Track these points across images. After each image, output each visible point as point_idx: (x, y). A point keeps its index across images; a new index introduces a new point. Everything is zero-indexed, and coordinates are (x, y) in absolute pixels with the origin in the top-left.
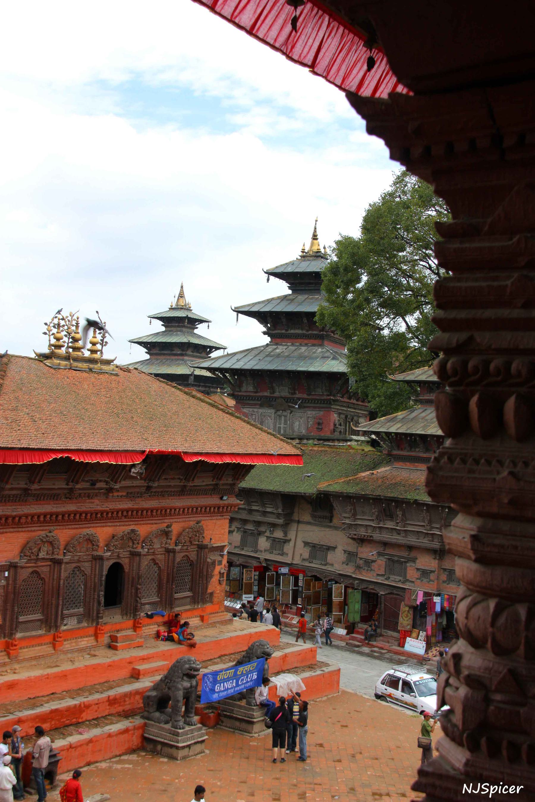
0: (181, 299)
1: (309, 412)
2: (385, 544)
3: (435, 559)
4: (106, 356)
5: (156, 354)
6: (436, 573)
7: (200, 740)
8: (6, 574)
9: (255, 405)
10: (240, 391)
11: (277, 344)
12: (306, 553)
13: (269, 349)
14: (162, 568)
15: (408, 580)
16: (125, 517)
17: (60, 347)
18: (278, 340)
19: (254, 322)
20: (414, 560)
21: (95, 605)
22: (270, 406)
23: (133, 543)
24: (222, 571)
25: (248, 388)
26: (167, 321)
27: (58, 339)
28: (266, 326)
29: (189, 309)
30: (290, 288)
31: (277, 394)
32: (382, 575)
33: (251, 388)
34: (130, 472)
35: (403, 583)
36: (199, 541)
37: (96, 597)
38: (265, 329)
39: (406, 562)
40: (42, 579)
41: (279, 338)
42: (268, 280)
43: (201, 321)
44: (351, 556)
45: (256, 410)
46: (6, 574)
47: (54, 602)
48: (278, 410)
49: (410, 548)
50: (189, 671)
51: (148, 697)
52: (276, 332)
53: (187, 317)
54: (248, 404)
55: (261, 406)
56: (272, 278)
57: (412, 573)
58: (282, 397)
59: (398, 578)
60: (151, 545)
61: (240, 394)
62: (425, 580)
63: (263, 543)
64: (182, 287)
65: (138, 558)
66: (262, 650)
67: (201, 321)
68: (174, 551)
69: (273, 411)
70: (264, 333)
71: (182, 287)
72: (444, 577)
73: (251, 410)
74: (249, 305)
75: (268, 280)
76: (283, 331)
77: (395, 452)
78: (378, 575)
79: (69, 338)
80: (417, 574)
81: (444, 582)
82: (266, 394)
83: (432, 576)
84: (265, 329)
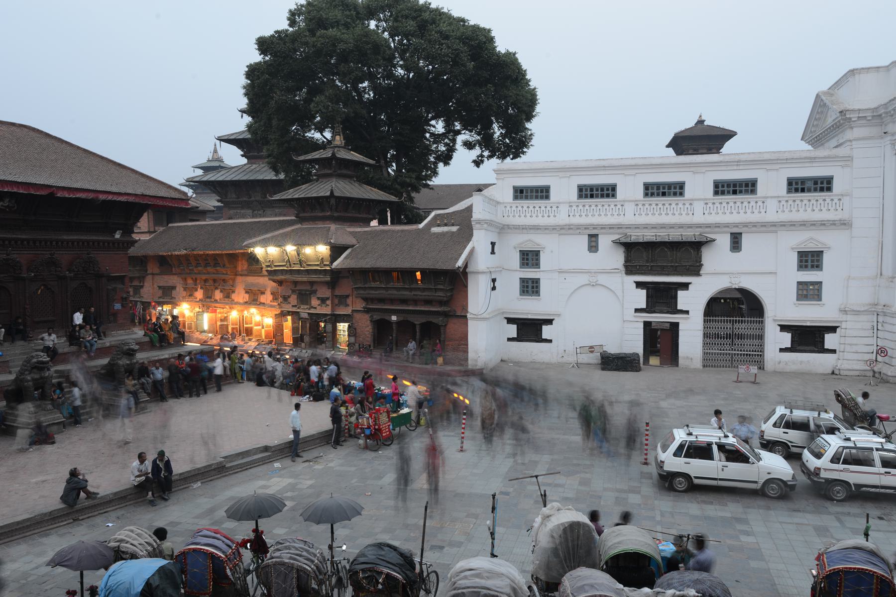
0: (215, 154)
1: (277, 210)
2: (296, 283)
3: (329, 288)
5: (200, 193)
6: (330, 299)
7: (56, 422)
9: (238, 207)
10: (227, 198)
11: (252, 163)
13: (246, 167)
15: (312, 307)
18: (253, 161)
20: (315, 292)
22: (249, 208)
25: (232, 197)
26: (206, 169)
29: (222, 161)
31: (253, 199)
32: (295, 306)
33: (234, 196)
35: (309, 309)
36: (94, 270)
38: (242, 153)
39: (310, 294)
41: (253, 159)
42: (242, 116)
45: (239, 211)
48: (254, 211)
49: (312, 283)
50: (36, 364)
51: (7, 391)
52: (251, 154)
54: (233, 208)
55: (242, 208)
58: (256, 201)
59: (306, 307)
60: (37, 272)
61: (227, 200)
62: (323, 305)
66: (127, 347)
69: (251, 211)
70: (242, 156)
72: (336, 301)
73: (235, 211)
74: (228, 135)
75: (242, 116)
76: (256, 154)
77: (301, 215)
78: (293, 306)
80: (318, 302)
81: (336, 305)
82: (245, 199)
83: (329, 302)
84: (242, 153)
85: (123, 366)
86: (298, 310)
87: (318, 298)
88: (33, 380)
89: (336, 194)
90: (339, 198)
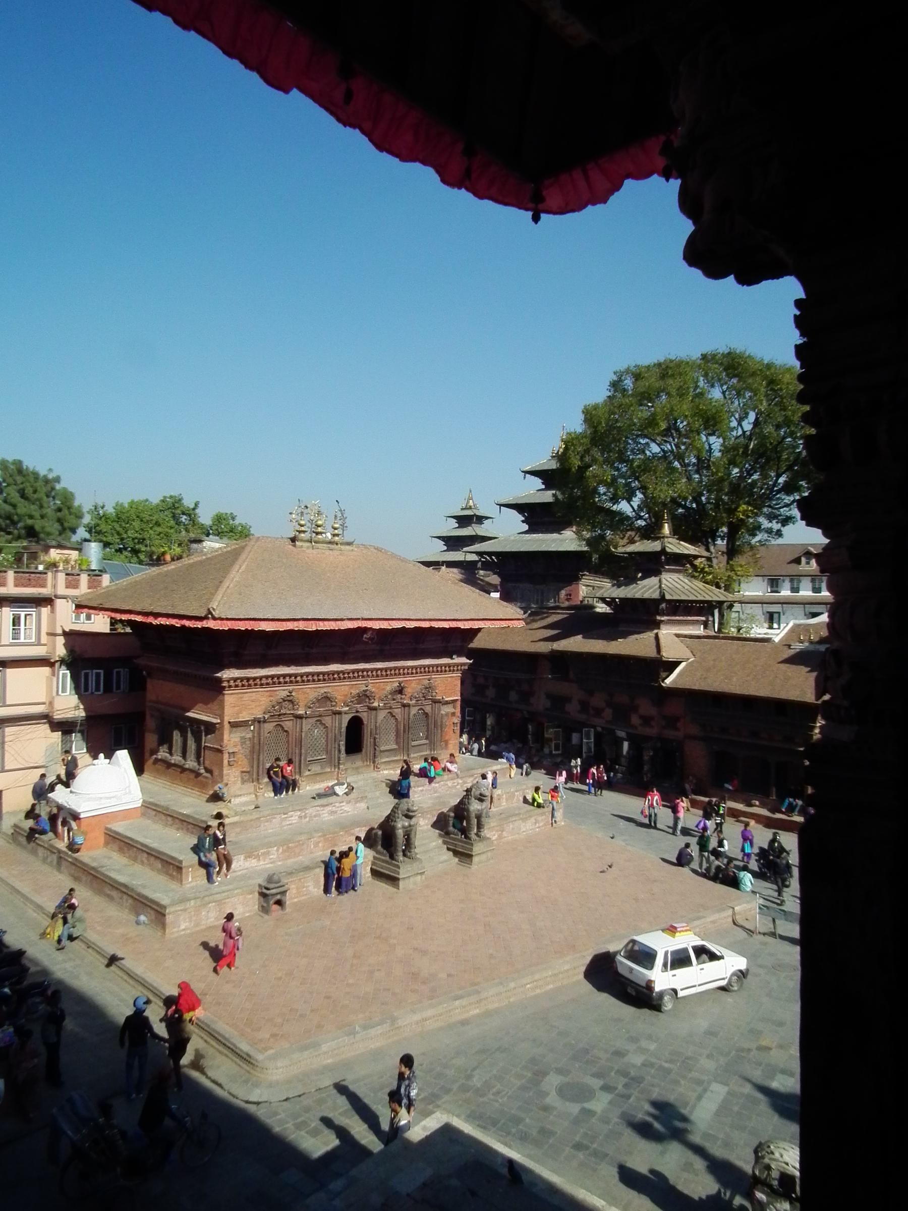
4: (347, 539)
8: (252, 728)
12: (548, 704)
14: (399, 720)
16: (363, 677)
17: (304, 532)
19: (514, 513)
21: (336, 752)
23: (370, 699)
24: (456, 721)
27: (302, 526)
28: (524, 516)
30: (543, 483)
34: (362, 636)
37: (337, 746)
38: (523, 519)
40: (286, 731)
43: (487, 518)
44: (584, 706)
46: (252, 728)
47: (297, 751)
53: (475, 515)
56: (528, 476)
57: (635, 720)
63: (513, 696)
64: (471, 491)
65: (375, 712)
67: (487, 518)
68: (408, 706)
70: (523, 522)
71: (471, 491)
79: (312, 524)
84: (523, 519)
85: (474, 810)
86: (614, 727)
87: (641, 717)
88: (404, 827)
89: (668, 597)
90: (669, 602)
